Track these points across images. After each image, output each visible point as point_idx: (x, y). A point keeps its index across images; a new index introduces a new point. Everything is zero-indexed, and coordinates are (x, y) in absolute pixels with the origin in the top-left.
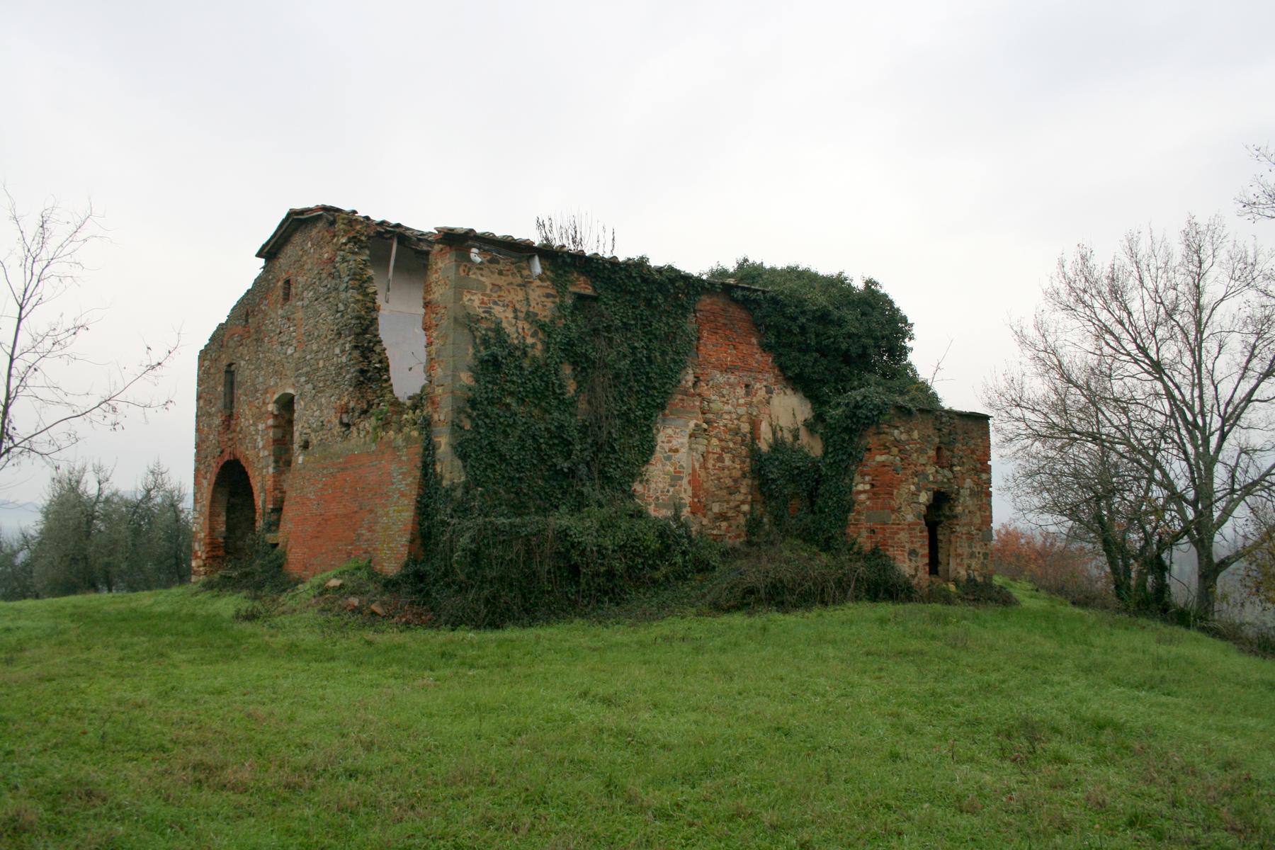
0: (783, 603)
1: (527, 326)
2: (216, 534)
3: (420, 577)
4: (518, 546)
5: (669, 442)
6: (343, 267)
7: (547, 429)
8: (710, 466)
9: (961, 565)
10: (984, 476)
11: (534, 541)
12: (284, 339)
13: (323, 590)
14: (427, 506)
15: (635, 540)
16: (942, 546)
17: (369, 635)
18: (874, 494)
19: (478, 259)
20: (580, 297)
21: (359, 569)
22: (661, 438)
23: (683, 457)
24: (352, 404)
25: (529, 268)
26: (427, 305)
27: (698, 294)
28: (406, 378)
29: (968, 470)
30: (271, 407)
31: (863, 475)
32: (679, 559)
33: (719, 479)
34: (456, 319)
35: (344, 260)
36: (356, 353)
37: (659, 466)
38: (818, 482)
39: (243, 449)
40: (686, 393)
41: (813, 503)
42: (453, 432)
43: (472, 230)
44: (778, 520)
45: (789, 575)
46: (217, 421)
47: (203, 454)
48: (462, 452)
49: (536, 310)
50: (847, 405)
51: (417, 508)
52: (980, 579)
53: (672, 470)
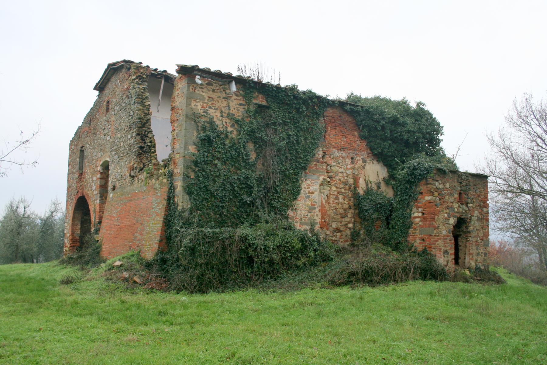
0: (372, 281)
1: (228, 121)
2: (75, 235)
3: (164, 261)
4: (217, 245)
5: (308, 188)
6: (133, 92)
7: (238, 179)
8: (331, 202)
9: (472, 259)
10: (485, 210)
11: (227, 242)
12: (106, 132)
13: (111, 268)
14: (170, 221)
15: (287, 243)
16: (461, 249)
17: (127, 297)
18: (424, 218)
19: (200, 82)
20: (260, 106)
21: (133, 256)
22: (304, 186)
23: (316, 197)
24: (135, 166)
25: (230, 89)
26: (173, 109)
27: (325, 107)
28: (162, 152)
29: (476, 206)
30: (99, 168)
31: (418, 208)
32: (312, 254)
33: (336, 209)
34: (187, 116)
35: (134, 88)
36: (138, 138)
37: (303, 201)
38: (391, 211)
39: (86, 190)
40: (318, 161)
41: (388, 224)
42: (184, 179)
43: (197, 66)
44: (368, 232)
45: (375, 265)
46: (76, 176)
47: (70, 193)
48: (188, 191)
49: (233, 113)
50: (409, 168)
51: (164, 222)
52: (482, 268)
53: (310, 203)
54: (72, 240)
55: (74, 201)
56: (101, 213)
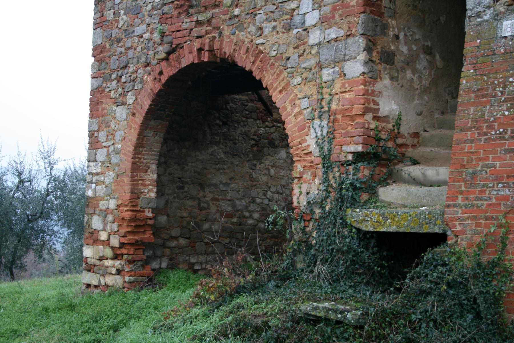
2: (141, 203)
47: (114, 63)
54: (131, 220)
55: (146, 87)
56: (369, 117)
